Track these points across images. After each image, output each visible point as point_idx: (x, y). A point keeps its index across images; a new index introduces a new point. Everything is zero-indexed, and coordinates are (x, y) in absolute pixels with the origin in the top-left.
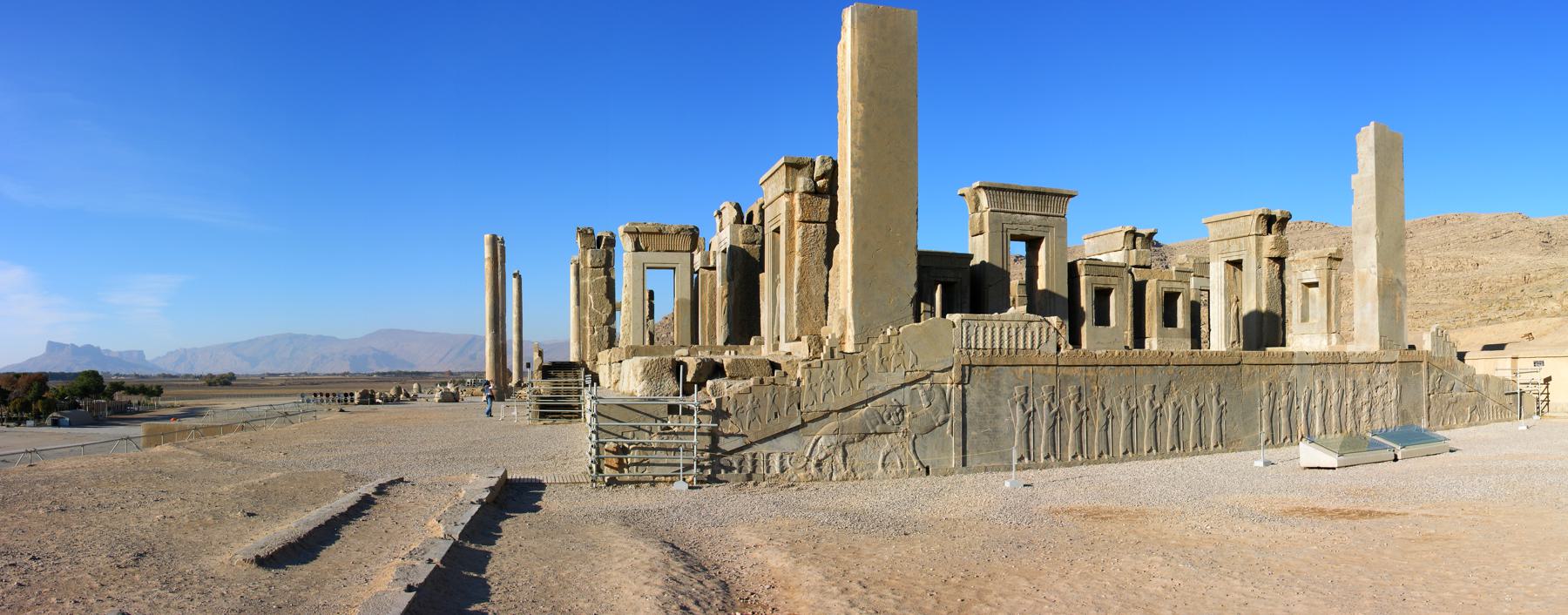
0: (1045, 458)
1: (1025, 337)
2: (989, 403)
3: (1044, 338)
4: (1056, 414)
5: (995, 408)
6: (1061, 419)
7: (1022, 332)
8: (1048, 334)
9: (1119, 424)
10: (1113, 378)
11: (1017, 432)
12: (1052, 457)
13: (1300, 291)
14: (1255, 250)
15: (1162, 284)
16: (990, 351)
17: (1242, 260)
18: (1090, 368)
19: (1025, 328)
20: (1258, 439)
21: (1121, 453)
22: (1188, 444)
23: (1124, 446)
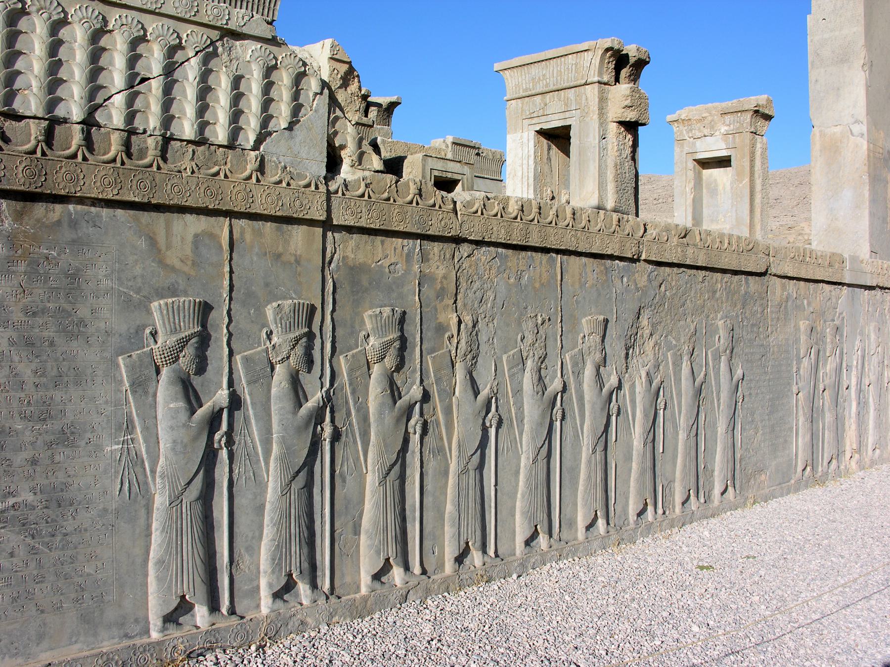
0: (277, 595)
1: (205, 91)
2: (26, 370)
3: (282, 111)
4: (318, 416)
5: (58, 395)
6: (336, 436)
7: (191, 71)
8: (296, 96)
9: (514, 445)
10: (502, 289)
11: (160, 500)
12: (303, 588)
13: (691, 174)
14: (596, 108)
15: (431, 163)
16: (36, 130)
17: (568, 128)
18: (436, 247)
19: (209, 56)
20: (790, 466)
21: (520, 540)
22: (672, 495)
23: (529, 515)
